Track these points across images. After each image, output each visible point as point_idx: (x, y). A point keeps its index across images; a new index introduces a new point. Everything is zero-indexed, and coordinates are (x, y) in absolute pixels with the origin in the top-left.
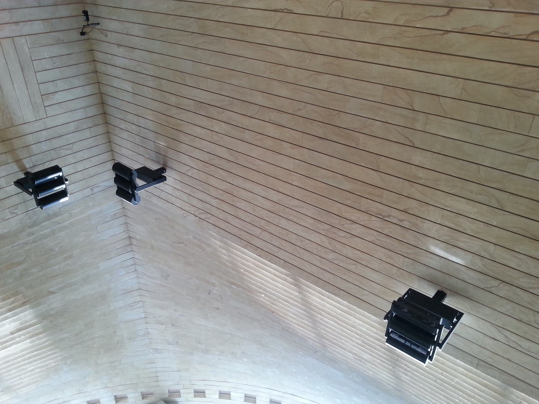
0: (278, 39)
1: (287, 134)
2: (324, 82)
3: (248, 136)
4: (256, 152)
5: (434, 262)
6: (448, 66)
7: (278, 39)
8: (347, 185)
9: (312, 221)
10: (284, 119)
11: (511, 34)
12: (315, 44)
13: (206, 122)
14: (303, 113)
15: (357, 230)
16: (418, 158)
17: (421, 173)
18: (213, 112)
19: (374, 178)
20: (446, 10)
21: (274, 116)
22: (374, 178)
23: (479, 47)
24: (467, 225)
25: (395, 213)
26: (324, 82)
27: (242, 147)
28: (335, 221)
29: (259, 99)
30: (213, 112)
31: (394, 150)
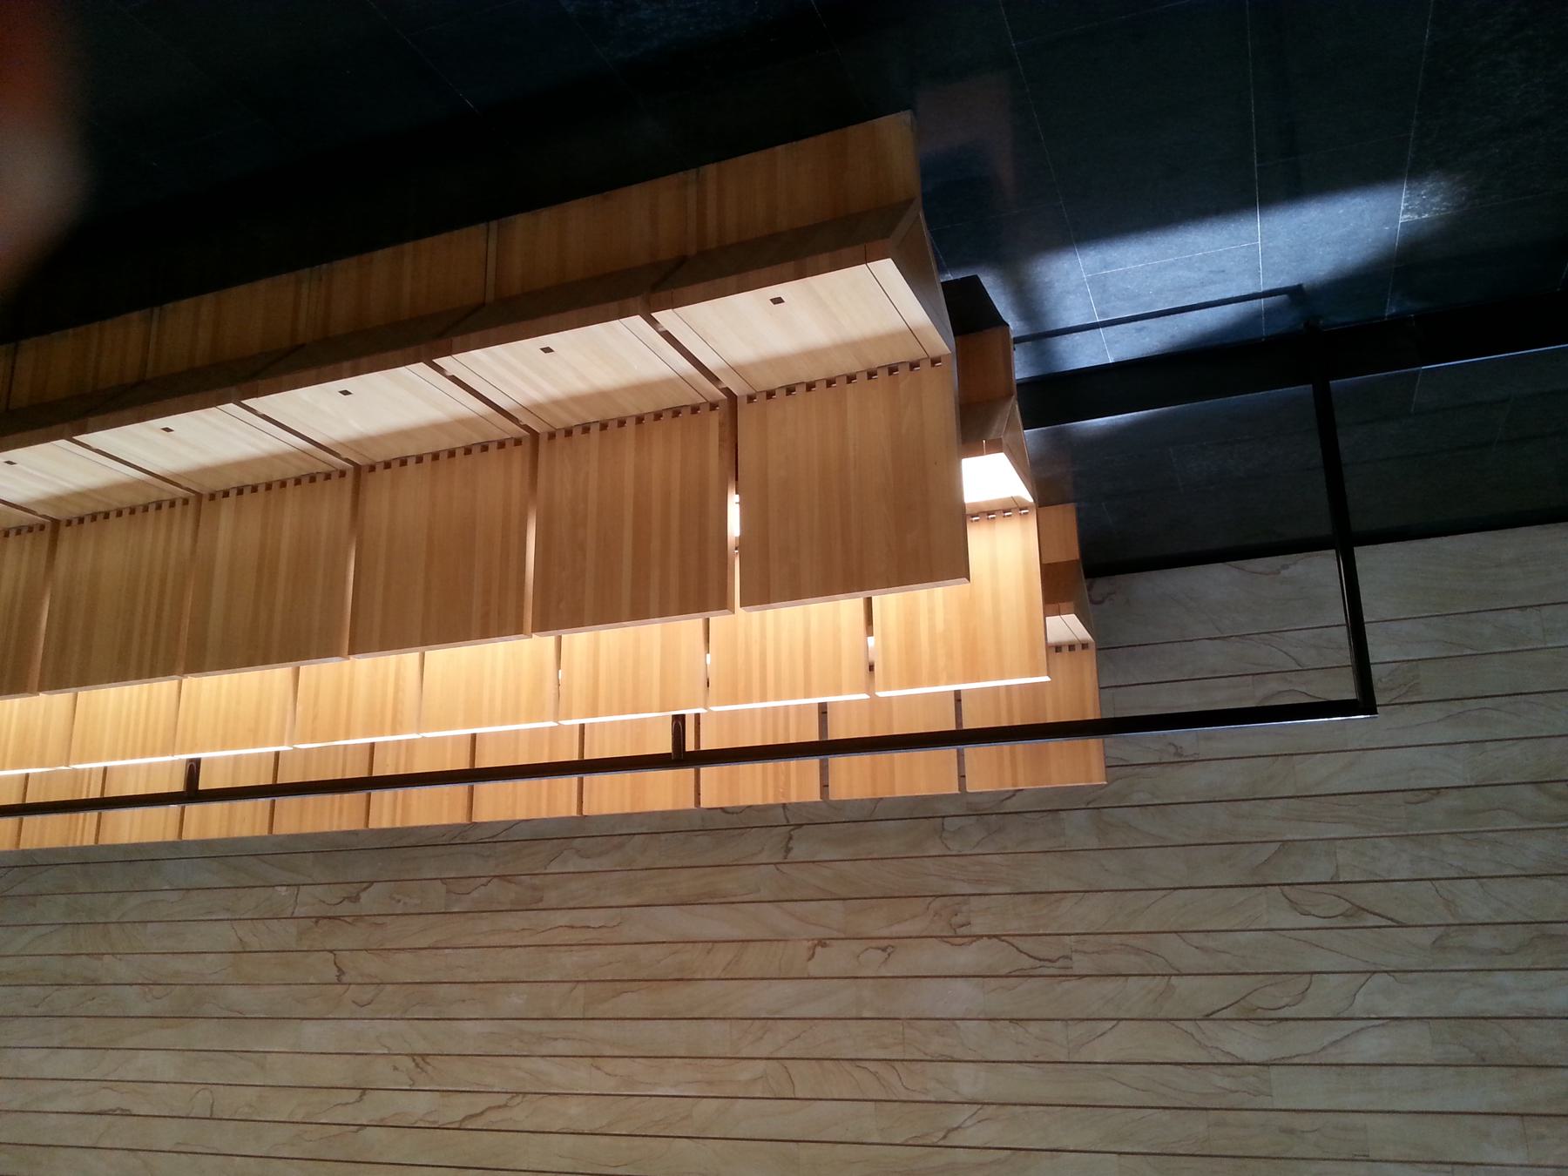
20: (357, 1093)
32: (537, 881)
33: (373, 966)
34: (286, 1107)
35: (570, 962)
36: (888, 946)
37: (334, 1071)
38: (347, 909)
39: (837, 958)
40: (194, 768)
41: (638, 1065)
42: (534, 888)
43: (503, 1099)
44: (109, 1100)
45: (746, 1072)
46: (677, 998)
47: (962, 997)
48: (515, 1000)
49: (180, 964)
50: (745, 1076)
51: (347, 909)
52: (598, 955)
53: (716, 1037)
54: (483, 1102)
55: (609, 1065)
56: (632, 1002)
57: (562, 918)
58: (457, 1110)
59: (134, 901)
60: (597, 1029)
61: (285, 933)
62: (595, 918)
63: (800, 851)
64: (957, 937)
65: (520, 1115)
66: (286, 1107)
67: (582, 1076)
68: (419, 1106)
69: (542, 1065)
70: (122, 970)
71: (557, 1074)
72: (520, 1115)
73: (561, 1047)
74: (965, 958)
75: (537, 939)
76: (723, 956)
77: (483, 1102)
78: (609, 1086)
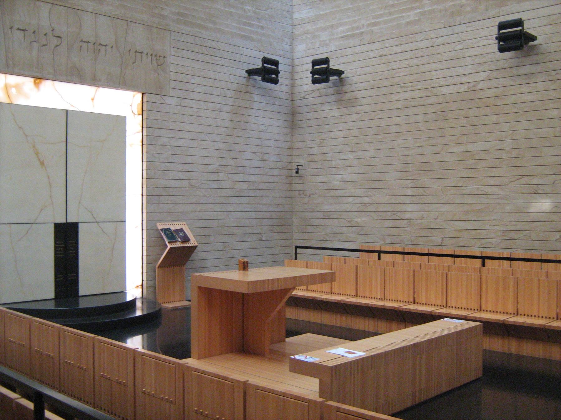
11: (528, 177)
17: (552, 106)
32: (504, 238)
35: (495, 217)
36: (422, 218)
39: (433, 216)
40: (483, 265)
41: (476, 193)
42: (505, 236)
43: (511, 184)
45: (452, 192)
46: (466, 208)
47: (409, 208)
48: (509, 208)
50: (452, 191)
52: (487, 218)
54: (516, 183)
55: (483, 193)
56: (478, 207)
57: (496, 228)
58: (523, 181)
60: (486, 201)
62: (487, 227)
63: (439, 240)
64: (410, 219)
65: (506, 180)
67: (489, 190)
68: (535, 181)
69: (500, 192)
71: (496, 190)
72: (506, 180)
73: (495, 197)
74: (408, 215)
75: (503, 223)
76: (456, 217)
77: (516, 183)
78: (483, 188)
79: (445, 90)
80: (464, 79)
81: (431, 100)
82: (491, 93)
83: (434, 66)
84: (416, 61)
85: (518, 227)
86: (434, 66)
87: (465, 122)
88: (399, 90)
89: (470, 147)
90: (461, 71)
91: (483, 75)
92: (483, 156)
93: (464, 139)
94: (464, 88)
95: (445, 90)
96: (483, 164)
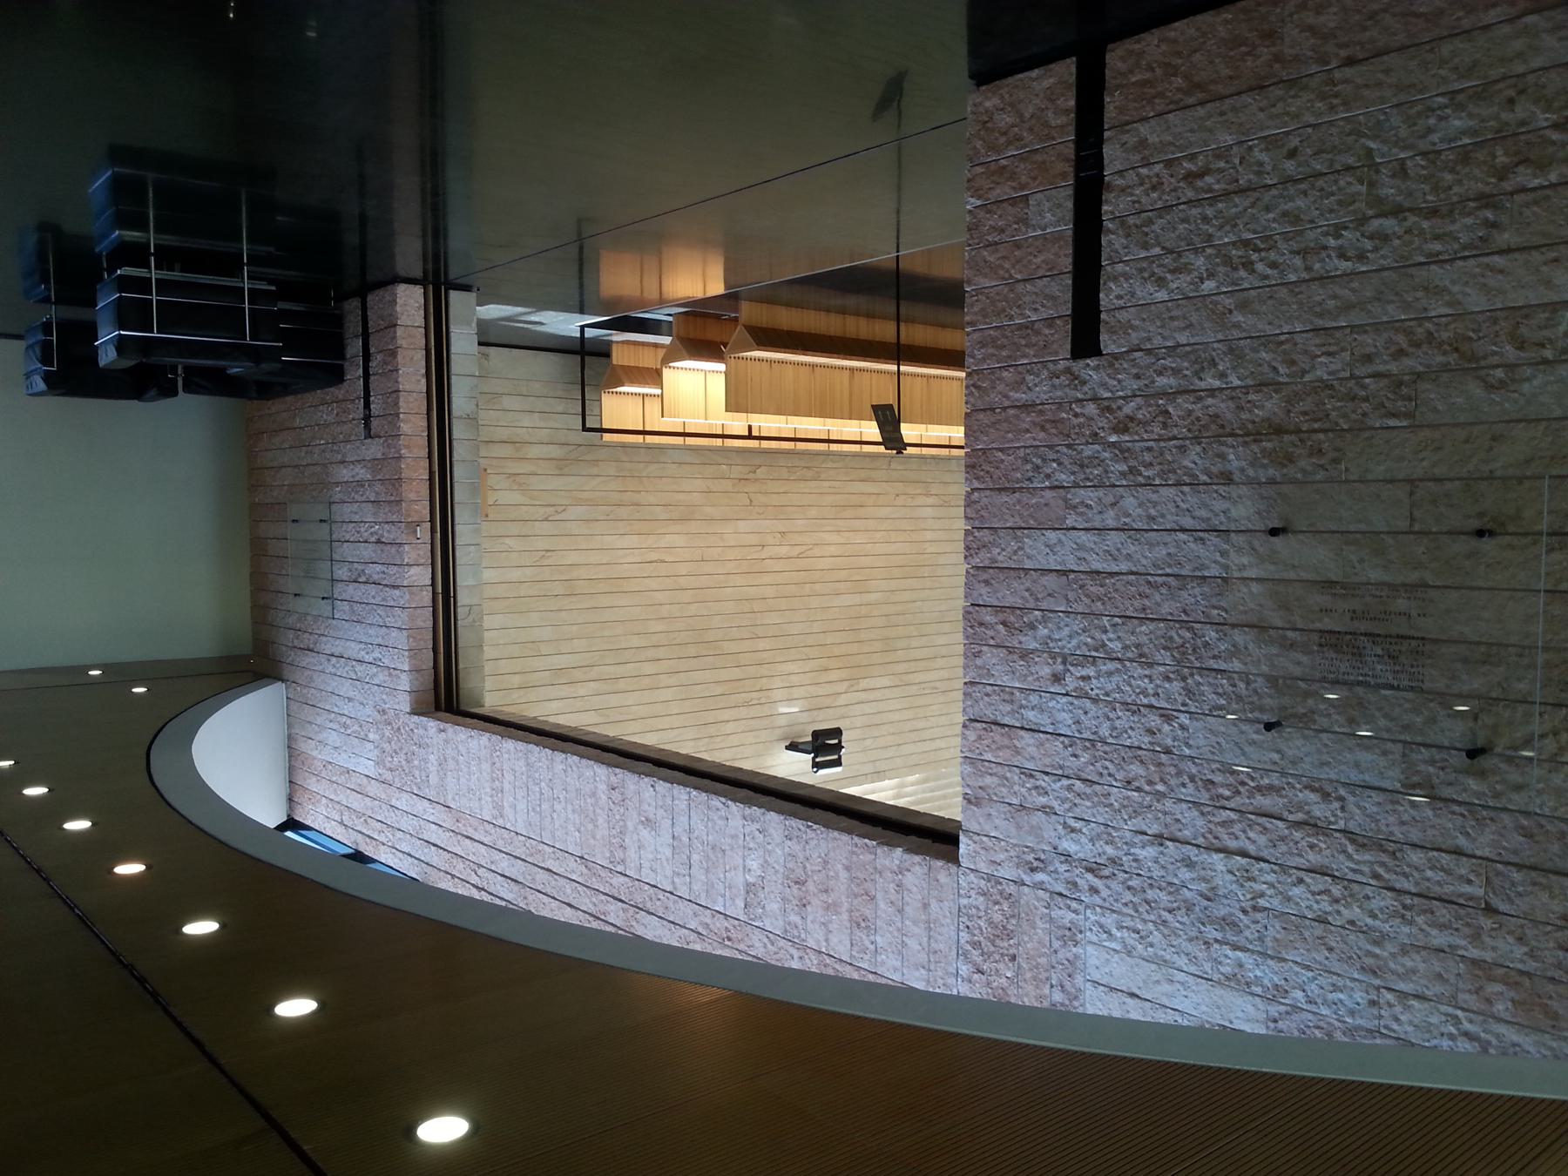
0: (653, 584)
1: (664, 666)
2: (693, 609)
3: (622, 685)
4: (631, 699)
5: (782, 721)
6: (767, 579)
7: (653, 584)
8: (719, 690)
9: (692, 743)
10: (661, 653)
12: (683, 582)
13: (565, 691)
14: (678, 641)
15: (730, 728)
16: (762, 644)
17: (765, 655)
18: (578, 675)
19: (737, 673)
21: (651, 653)
22: (737, 673)
23: (779, 566)
24: (795, 679)
25: (755, 695)
26: (693, 609)
27: (614, 700)
28: (712, 730)
29: (635, 642)
30: (578, 675)
31: (747, 646)
33: (763, 499)
34: (732, 554)
36: (913, 496)
37: (753, 539)
38: (751, 476)
39: (900, 501)
44: (654, 556)
47: (929, 512)
48: (813, 512)
49: (681, 496)
51: (751, 476)
52: (838, 497)
53: (871, 524)
56: (849, 513)
57: (827, 484)
58: (796, 551)
59: (652, 467)
60: (840, 522)
61: (727, 485)
63: (893, 465)
65: (817, 551)
66: (732, 554)
67: (834, 538)
68: (784, 551)
70: (652, 499)
72: (817, 551)
74: (930, 501)
79: (885, 682)
80: (863, 696)
81: (901, 668)
82: (833, 676)
83: (897, 716)
84: (920, 724)
85: (802, 484)
86: (897, 716)
87: (863, 636)
88: (938, 684)
89: (856, 599)
90: (867, 708)
91: (842, 700)
92: (842, 586)
93: (864, 610)
94: (864, 684)
95: (885, 682)
96: (843, 575)
